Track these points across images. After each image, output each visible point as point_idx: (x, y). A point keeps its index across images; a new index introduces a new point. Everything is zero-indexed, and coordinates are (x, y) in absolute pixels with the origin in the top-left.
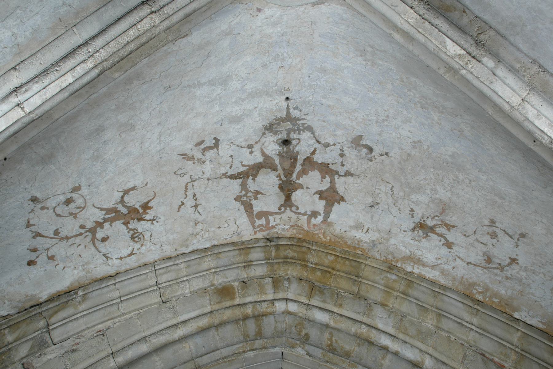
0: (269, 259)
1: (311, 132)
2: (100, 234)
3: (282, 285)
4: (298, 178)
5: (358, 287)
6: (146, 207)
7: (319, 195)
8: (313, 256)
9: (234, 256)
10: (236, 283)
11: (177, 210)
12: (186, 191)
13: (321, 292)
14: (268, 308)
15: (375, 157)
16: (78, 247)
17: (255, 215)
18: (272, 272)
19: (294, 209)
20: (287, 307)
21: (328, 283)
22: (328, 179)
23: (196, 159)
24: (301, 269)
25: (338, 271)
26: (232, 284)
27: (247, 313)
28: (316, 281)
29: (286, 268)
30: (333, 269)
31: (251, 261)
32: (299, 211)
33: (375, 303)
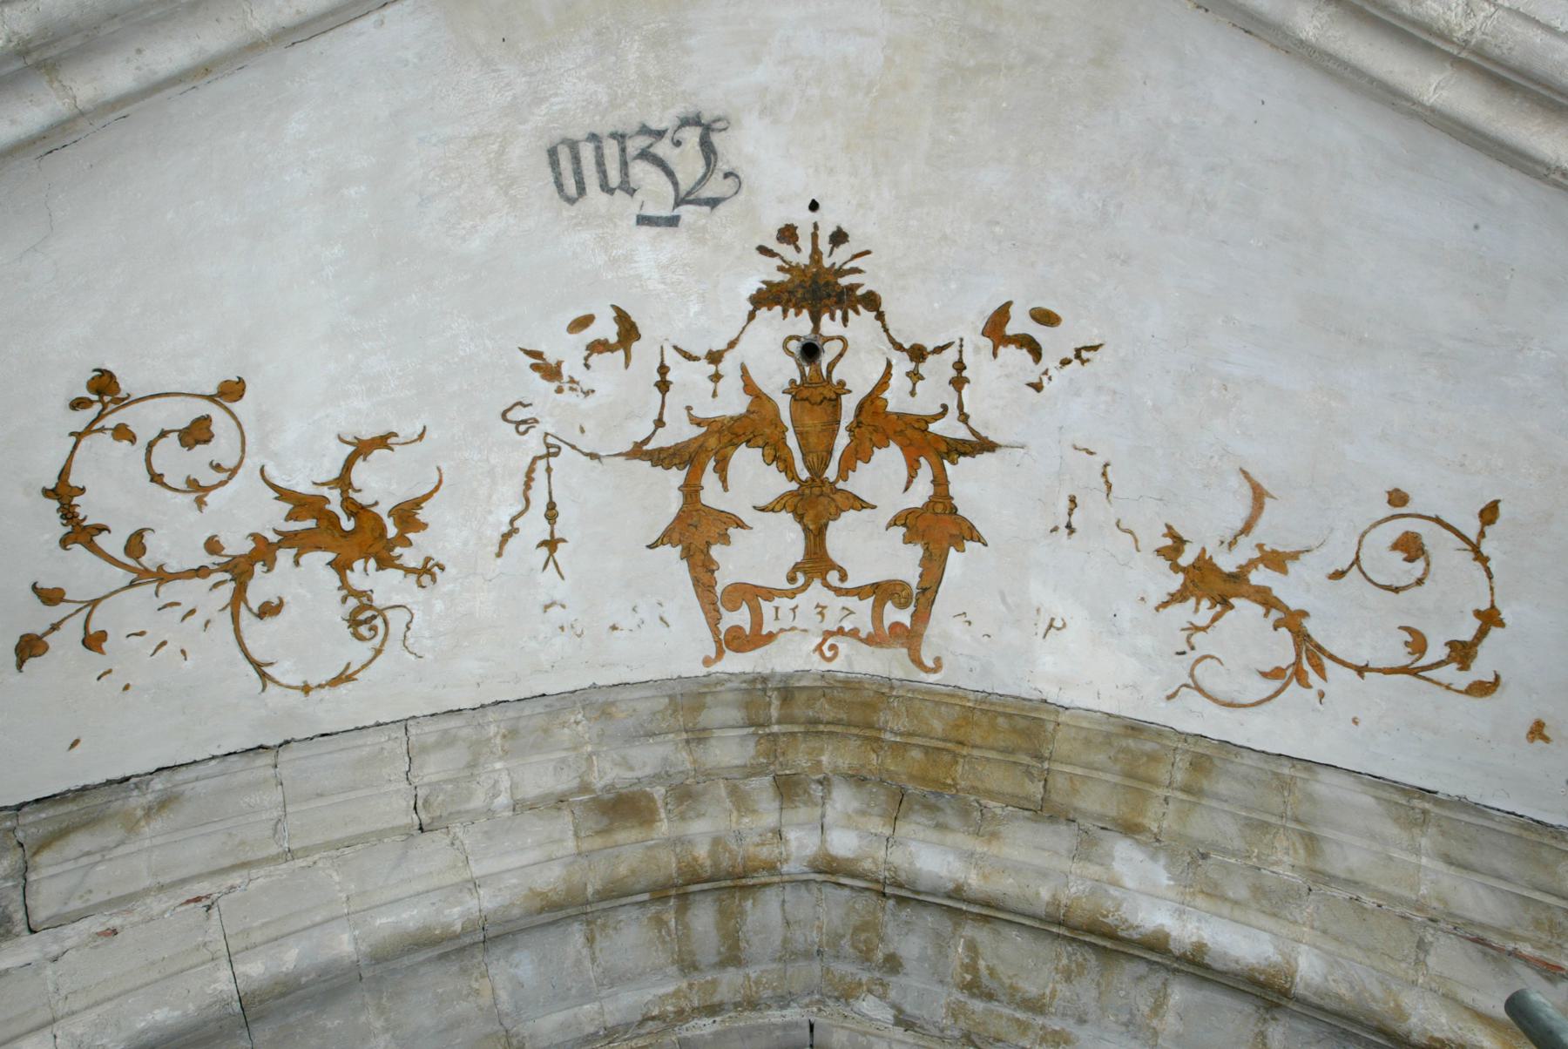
0: (762, 725)
1: (875, 313)
2: (262, 587)
3: (806, 791)
4: (843, 475)
5: (1042, 783)
6: (407, 514)
7: (904, 525)
8: (897, 715)
9: (654, 714)
10: (658, 788)
11: (496, 549)
12: (528, 486)
13: (932, 808)
14: (763, 844)
15: (1050, 373)
16: (183, 619)
17: (719, 595)
18: (772, 759)
19: (833, 577)
20: (823, 842)
21: (949, 781)
22: (925, 472)
23: (566, 378)
24: (861, 745)
25: (974, 746)
26: (648, 789)
27: (695, 859)
28: (912, 777)
29: (817, 745)
30: (961, 743)
31: (704, 730)
32: (848, 585)
33: (1102, 828)
